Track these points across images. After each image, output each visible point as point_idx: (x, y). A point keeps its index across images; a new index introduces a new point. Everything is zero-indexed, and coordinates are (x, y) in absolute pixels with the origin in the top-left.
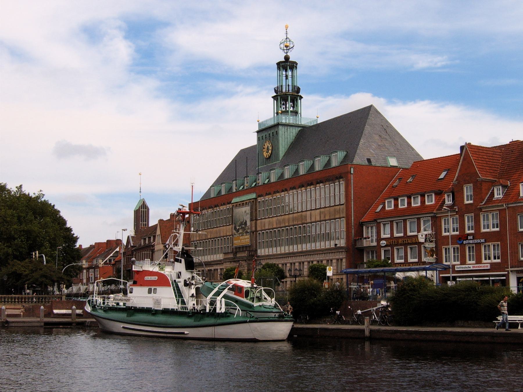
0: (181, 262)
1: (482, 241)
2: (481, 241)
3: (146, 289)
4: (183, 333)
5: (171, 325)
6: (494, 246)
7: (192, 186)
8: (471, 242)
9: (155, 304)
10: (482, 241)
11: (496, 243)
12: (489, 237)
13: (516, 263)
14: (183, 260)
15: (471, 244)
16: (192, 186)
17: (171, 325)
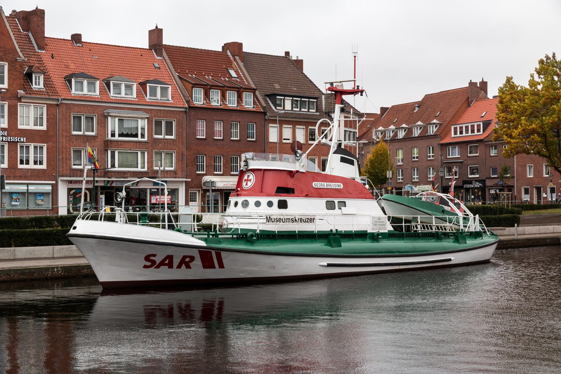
0: (353, 165)
1: (22, 139)
2: (20, 139)
3: (322, 202)
4: (450, 260)
5: (431, 251)
6: (35, 147)
7: (355, 57)
8: (4, 139)
9: (376, 225)
10: (22, 139)
11: (39, 145)
12: (31, 135)
13: (68, 172)
14: (355, 161)
15: (4, 141)
16: (355, 57)
17: (431, 251)
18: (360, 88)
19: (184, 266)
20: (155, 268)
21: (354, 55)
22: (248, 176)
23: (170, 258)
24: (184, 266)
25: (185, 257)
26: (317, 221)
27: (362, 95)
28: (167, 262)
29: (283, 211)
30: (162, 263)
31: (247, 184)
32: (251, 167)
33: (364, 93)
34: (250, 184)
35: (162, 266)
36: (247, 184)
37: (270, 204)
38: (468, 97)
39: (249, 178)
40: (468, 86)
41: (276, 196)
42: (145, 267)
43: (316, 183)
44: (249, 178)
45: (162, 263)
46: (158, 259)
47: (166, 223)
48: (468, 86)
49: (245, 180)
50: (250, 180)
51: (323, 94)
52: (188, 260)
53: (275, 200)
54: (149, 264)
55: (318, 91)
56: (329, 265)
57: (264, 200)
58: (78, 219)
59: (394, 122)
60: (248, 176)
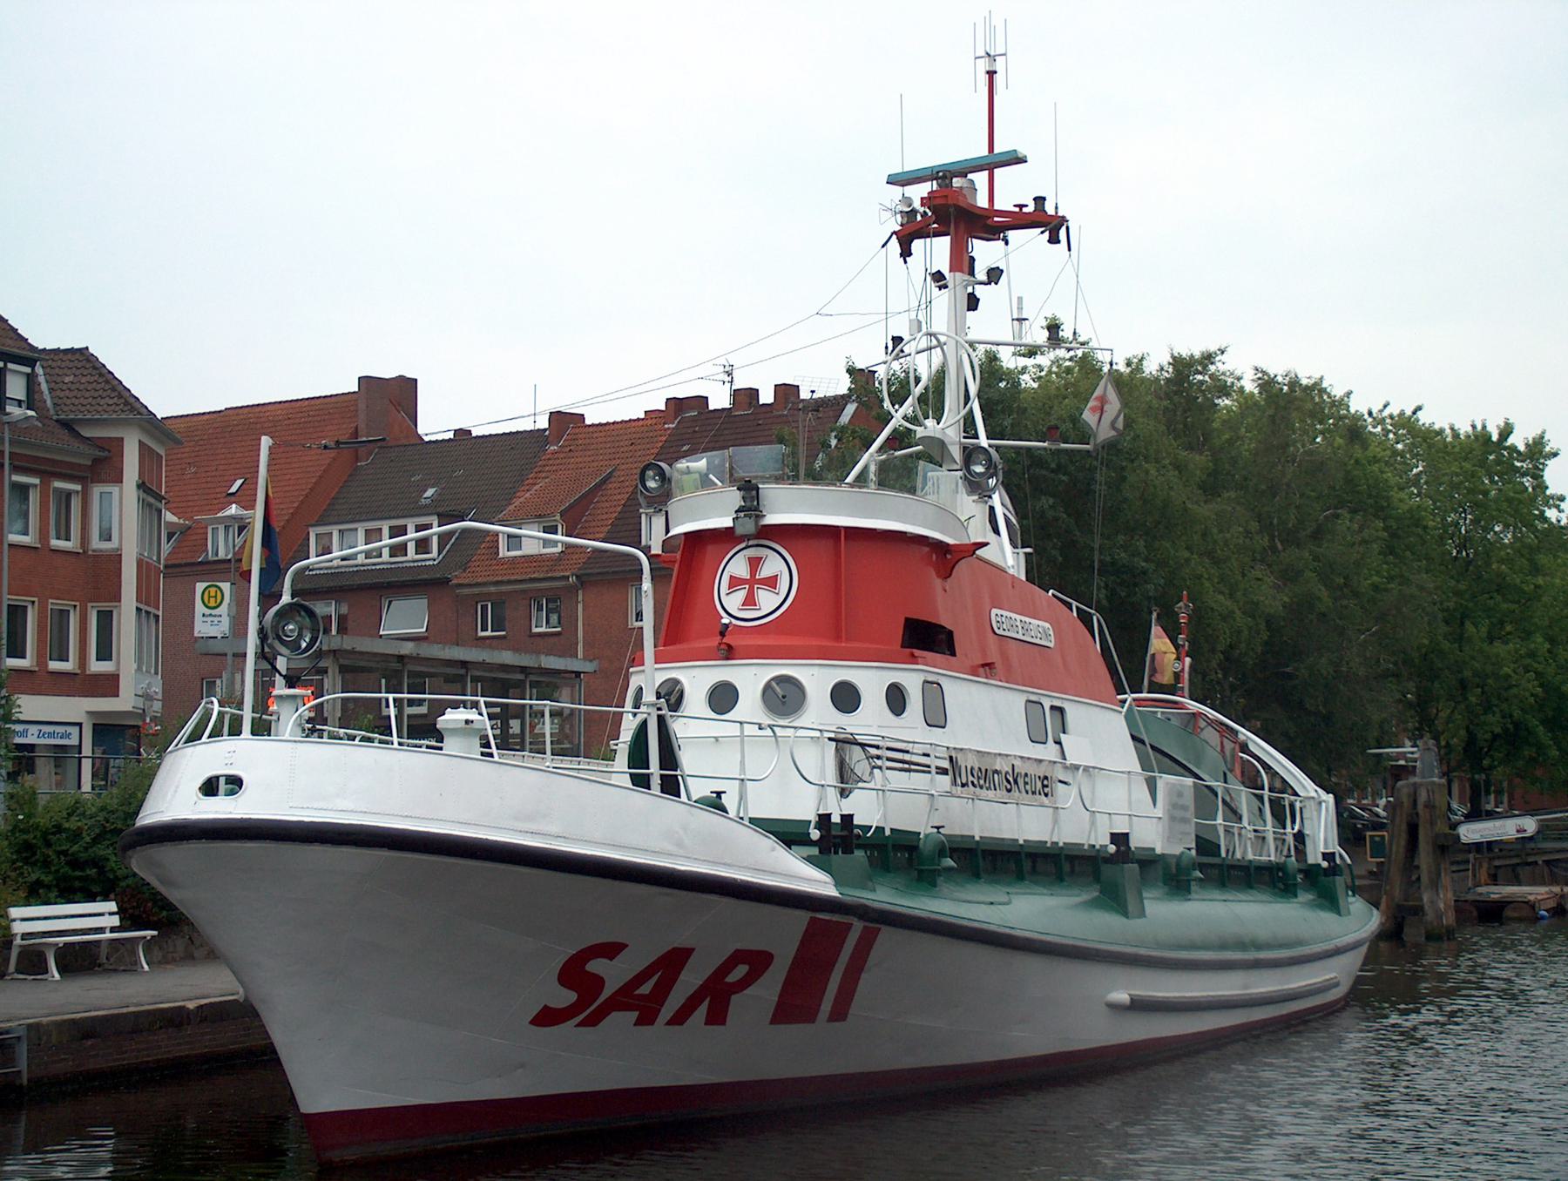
7: (991, 74)
16: (991, 74)
18: (1049, 209)
19: (702, 1011)
20: (579, 1025)
21: (983, 66)
22: (755, 563)
23: (675, 960)
24: (702, 1011)
25: (738, 957)
26: (1066, 796)
27: (1054, 240)
28: (645, 989)
29: (936, 736)
30: (624, 999)
31: (750, 601)
32: (772, 519)
33: (1063, 232)
34: (768, 601)
35: (614, 1014)
36: (750, 601)
37: (896, 699)
38: (356, 428)
39: (766, 572)
40: (356, 389)
41: (913, 659)
42: (547, 1017)
43: (1000, 612)
44: (766, 572)
45: (624, 999)
46: (613, 974)
47: (654, 768)
48: (356, 389)
49: (735, 582)
50: (772, 582)
51: (33, 349)
52: (741, 971)
53: (911, 680)
54: (567, 997)
55: (12, 334)
56: (1139, 1006)
57: (871, 680)
58: (195, 737)
59: (233, 489)
60: (755, 563)
